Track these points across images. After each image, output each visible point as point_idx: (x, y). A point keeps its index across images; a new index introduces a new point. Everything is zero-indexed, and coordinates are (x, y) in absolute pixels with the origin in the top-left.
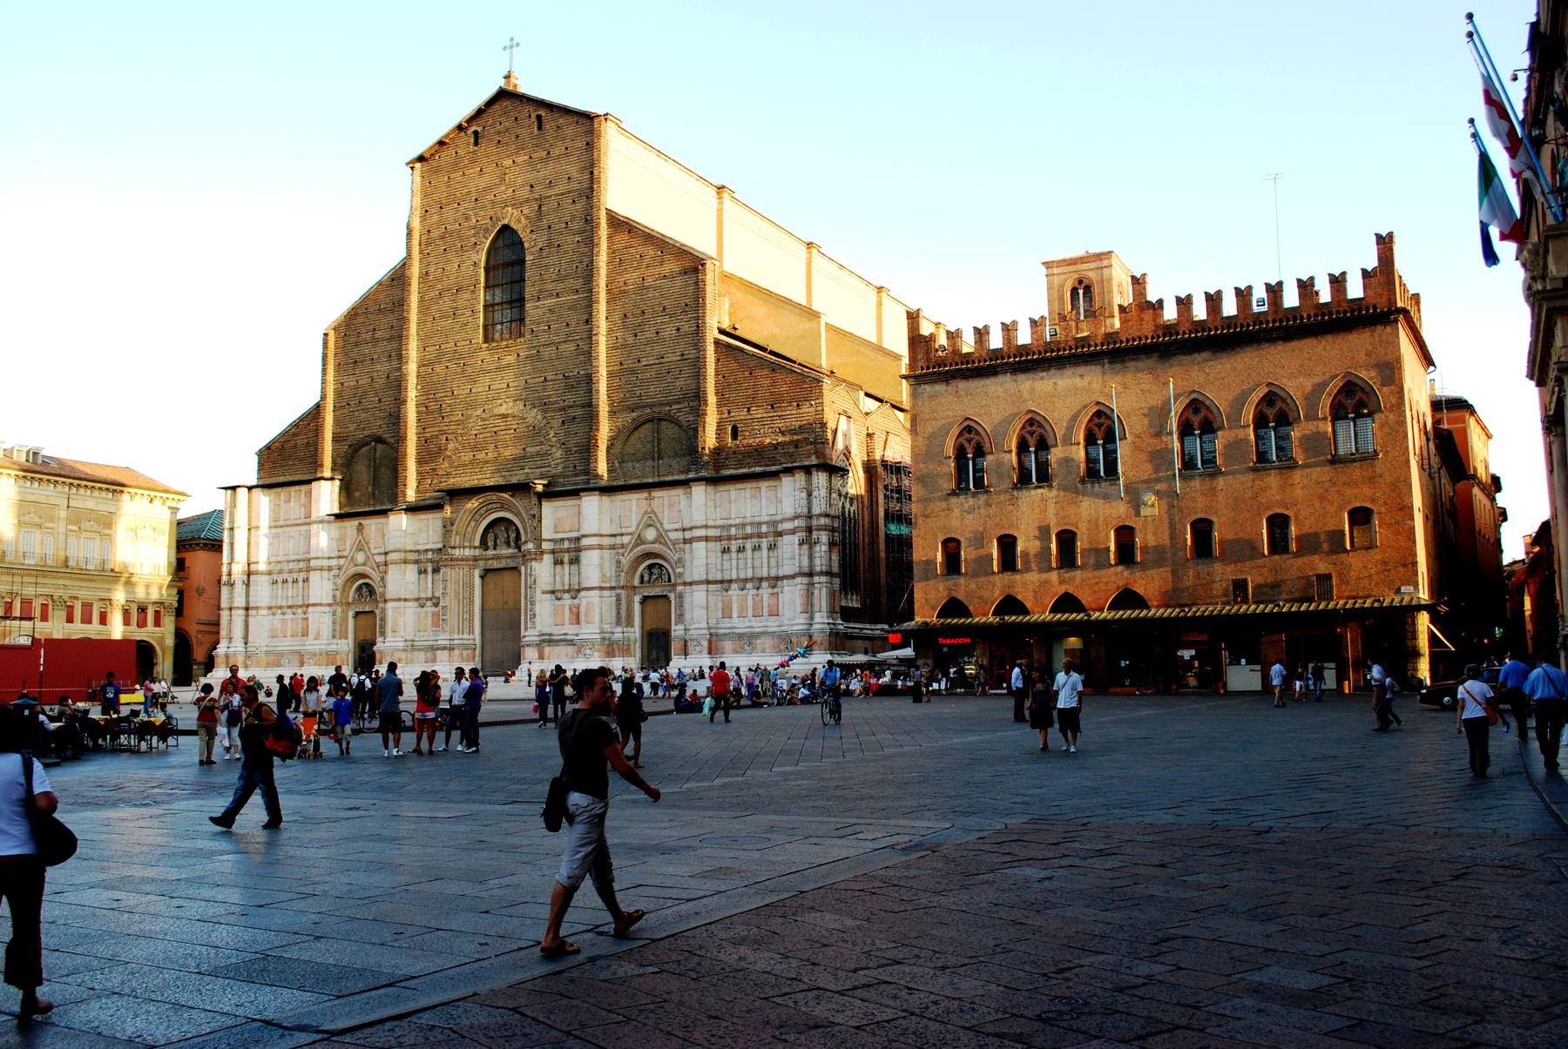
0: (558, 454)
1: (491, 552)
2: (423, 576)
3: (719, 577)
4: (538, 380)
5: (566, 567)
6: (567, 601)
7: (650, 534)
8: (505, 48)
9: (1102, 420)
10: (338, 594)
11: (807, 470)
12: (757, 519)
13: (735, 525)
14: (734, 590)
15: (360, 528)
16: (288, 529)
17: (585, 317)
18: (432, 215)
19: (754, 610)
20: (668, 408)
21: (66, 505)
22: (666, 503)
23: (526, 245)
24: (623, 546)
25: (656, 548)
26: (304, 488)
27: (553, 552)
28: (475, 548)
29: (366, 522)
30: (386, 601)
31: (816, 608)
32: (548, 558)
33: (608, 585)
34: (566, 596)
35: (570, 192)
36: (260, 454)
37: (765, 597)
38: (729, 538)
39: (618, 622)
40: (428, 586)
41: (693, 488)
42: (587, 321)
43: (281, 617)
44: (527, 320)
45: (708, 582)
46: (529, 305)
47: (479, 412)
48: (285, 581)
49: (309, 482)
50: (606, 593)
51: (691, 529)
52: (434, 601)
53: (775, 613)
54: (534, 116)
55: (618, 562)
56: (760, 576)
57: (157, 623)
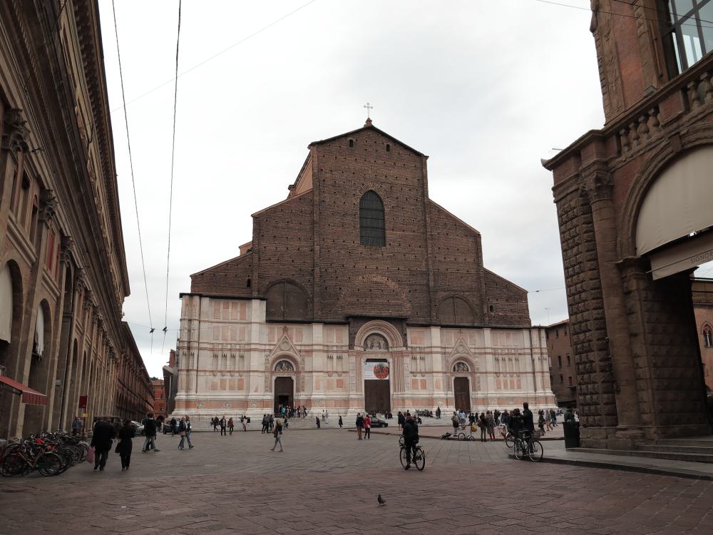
0: (409, 305)
6: (419, 377)
8: (365, 107)
12: (509, 347)
16: (227, 325)
22: (468, 336)
24: (449, 353)
25: (464, 355)
27: (412, 353)
29: (289, 326)
30: (306, 372)
36: (194, 277)
37: (515, 381)
39: (449, 389)
43: (221, 377)
44: (387, 239)
46: (387, 232)
47: (360, 278)
54: (386, 144)
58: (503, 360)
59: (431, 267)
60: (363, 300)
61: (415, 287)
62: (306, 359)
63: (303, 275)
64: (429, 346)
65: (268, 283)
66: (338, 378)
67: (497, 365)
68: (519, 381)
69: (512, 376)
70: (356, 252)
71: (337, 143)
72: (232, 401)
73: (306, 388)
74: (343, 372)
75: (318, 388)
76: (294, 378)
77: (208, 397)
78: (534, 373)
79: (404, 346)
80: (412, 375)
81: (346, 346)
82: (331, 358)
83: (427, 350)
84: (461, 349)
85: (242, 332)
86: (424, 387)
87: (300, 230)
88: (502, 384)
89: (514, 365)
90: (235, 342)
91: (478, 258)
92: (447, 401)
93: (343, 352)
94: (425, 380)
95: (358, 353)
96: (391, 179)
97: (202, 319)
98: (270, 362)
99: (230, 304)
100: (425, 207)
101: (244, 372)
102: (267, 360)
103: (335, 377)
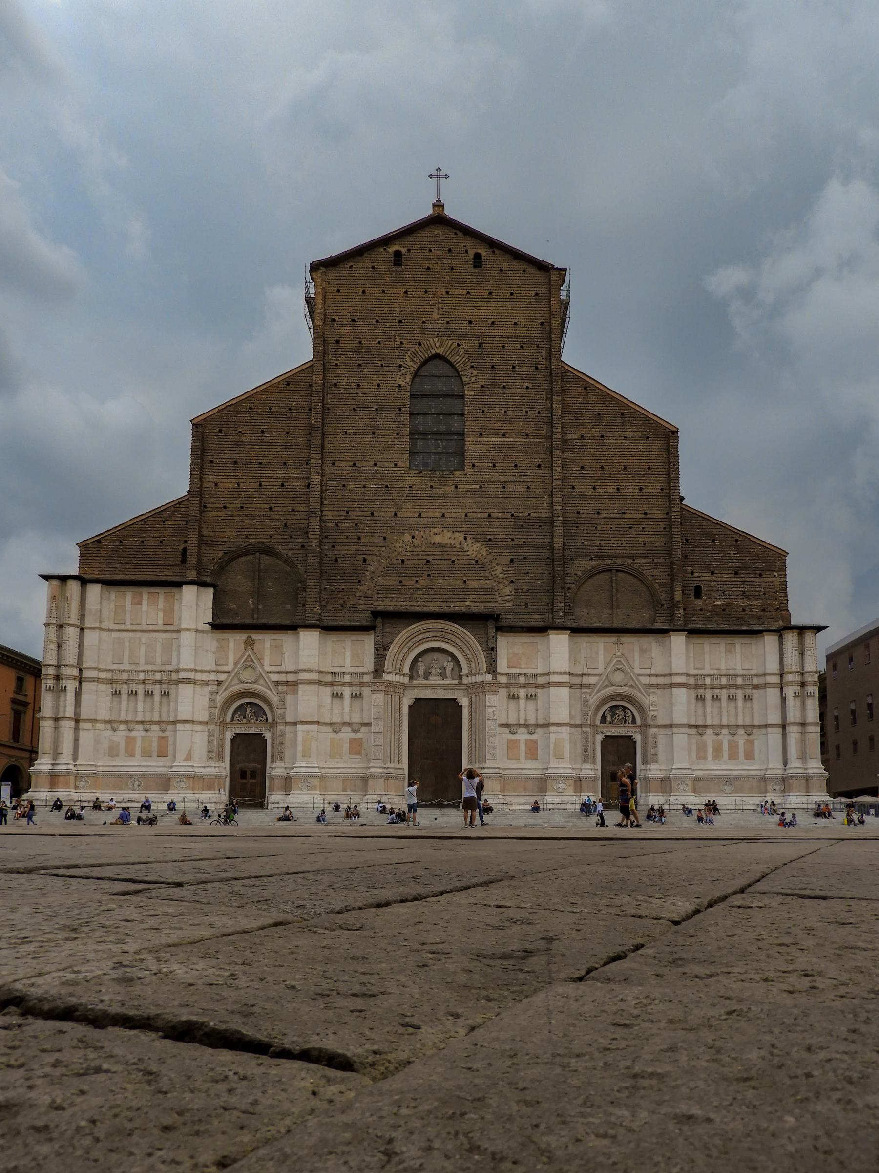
0: (508, 590)
2: (336, 701)
3: (693, 723)
6: (522, 736)
8: (431, 176)
12: (731, 672)
13: (709, 676)
14: (709, 737)
15: (249, 643)
16: (138, 635)
17: (538, 461)
18: (342, 325)
19: (729, 754)
20: (630, 561)
23: (464, 379)
24: (589, 686)
26: (162, 592)
27: (508, 686)
28: (404, 675)
29: (256, 636)
30: (286, 724)
32: (503, 692)
33: (572, 723)
35: (516, 337)
38: (705, 687)
39: (586, 757)
40: (345, 710)
41: (672, 637)
42: (539, 466)
44: (468, 455)
45: (690, 726)
47: (407, 537)
48: (133, 694)
50: (573, 730)
51: (664, 676)
52: (355, 726)
53: (750, 757)
54: (471, 253)
55: (585, 702)
58: (716, 698)
59: (558, 507)
60: (412, 582)
61: (523, 552)
62: (289, 699)
63: (291, 537)
64: (546, 671)
65: (221, 554)
66: (353, 736)
67: (700, 710)
68: (751, 743)
69: (734, 734)
70: (400, 484)
71: (367, 261)
72: (145, 776)
73: (287, 754)
74: (363, 725)
75: (306, 755)
76: (268, 735)
77: (101, 769)
78: (784, 727)
79: (488, 672)
80: (507, 730)
81: (368, 673)
82: (338, 696)
83: (541, 680)
84: (618, 677)
85: (168, 648)
86: (532, 752)
87: (285, 446)
88: (710, 750)
89: (740, 710)
90: (154, 668)
91: (669, 483)
92: (578, 783)
93: (363, 684)
94: (535, 742)
95: (389, 684)
96: (480, 328)
98: (219, 705)
99: (145, 597)
100: (552, 383)
101: (169, 722)
103: (346, 734)
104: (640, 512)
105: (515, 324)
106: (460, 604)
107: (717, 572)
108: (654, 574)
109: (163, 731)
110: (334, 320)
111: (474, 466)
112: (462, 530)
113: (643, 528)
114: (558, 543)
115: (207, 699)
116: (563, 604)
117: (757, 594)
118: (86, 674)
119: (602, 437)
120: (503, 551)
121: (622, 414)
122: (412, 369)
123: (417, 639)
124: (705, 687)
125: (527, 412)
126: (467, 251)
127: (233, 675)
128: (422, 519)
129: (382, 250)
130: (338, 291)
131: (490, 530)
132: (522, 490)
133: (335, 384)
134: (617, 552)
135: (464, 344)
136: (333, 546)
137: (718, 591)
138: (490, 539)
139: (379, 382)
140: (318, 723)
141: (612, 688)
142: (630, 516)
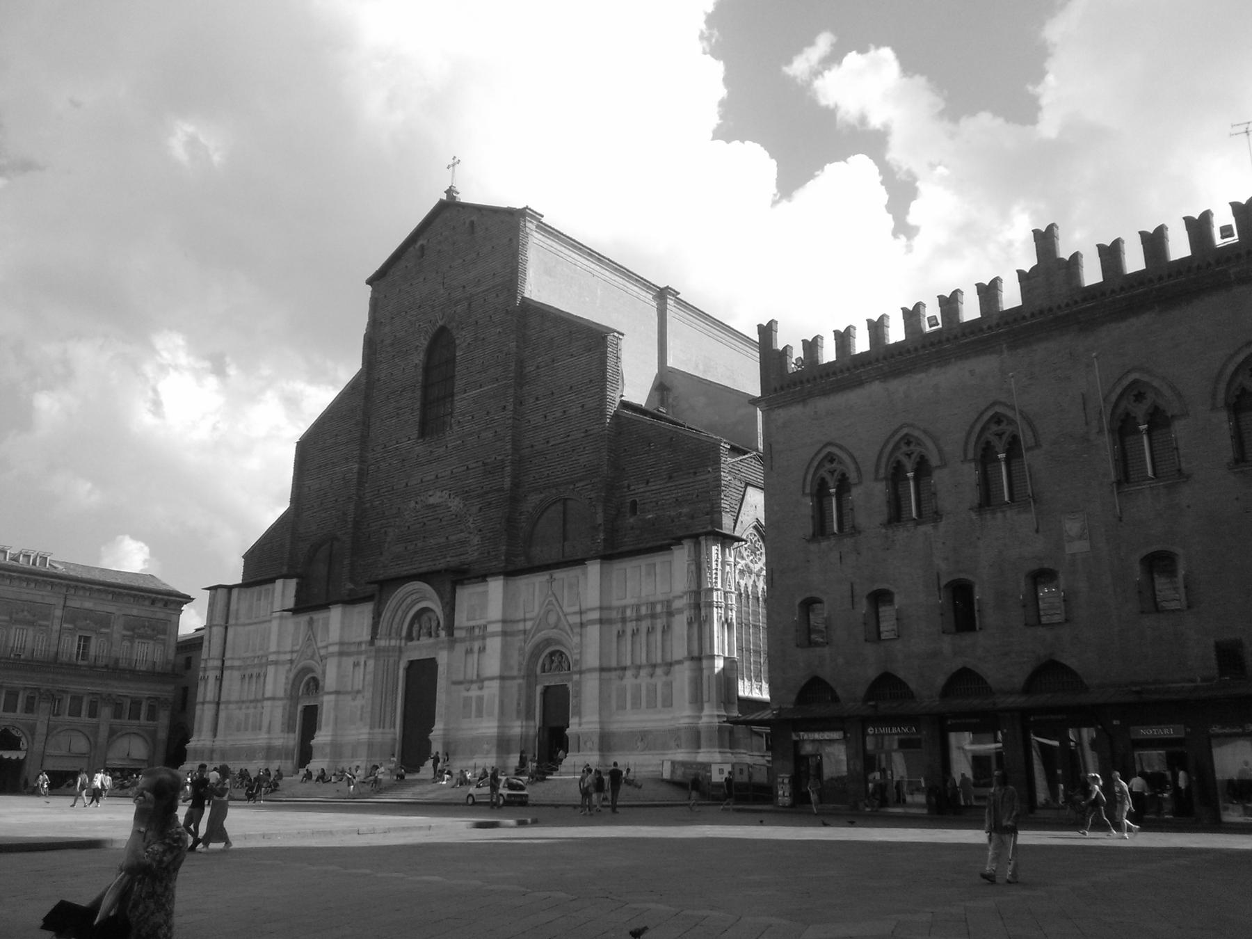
0: (476, 540)
1: (415, 643)
3: (614, 664)
4: (460, 469)
5: (476, 656)
6: (474, 693)
7: (552, 619)
9: (1003, 426)
10: (289, 687)
11: (695, 538)
12: (652, 599)
13: (629, 606)
14: (629, 680)
20: (571, 487)
21: (62, 603)
23: (457, 342)
24: (525, 632)
25: (553, 633)
26: (269, 586)
28: (401, 639)
31: (705, 698)
32: (460, 648)
34: (474, 686)
35: (493, 287)
38: (624, 620)
41: (590, 568)
47: (412, 504)
49: (272, 581)
50: (508, 683)
53: (668, 703)
54: (468, 222)
56: (654, 662)
57: (152, 715)
68: (669, 685)
80: (462, 687)
82: (356, 665)
95: (378, 650)
97: (232, 621)
98: (291, 682)
99: (263, 592)
102: (287, 678)
103: (360, 702)
104: (582, 431)
105: (494, 274)
106: (442, 561)
107: (652, 480)
108: (591, 496)
109: (263, 708)
110: (382, 322)
111: (459, 422)
112: (448, 487)
113: (584, 448)
114: (507, 483)
115: (284, 677)
116: (504, 547)
117: (690, 497)
118: (227, 663)
119: (553, 361)
120: (473, 501)
121: (570, 332)
122: (425, 346)
123: (409, 600)
124: (624, 620)
125: (498, 357)
126: (465, 223)
127: (300, 654)
128: (423, 484)
129: (412, 249)
130: (385, 296)
131: (467, 482)
132: (491, 435)
133: (379, 378)
134: (562, 479)
135: (459, 309)
136: (368, 525)
137: (651, 502)
138: (467, 492)
139: (403, 366)
140: (337, 693)
141: (543, 632)
142: (573, 437)
